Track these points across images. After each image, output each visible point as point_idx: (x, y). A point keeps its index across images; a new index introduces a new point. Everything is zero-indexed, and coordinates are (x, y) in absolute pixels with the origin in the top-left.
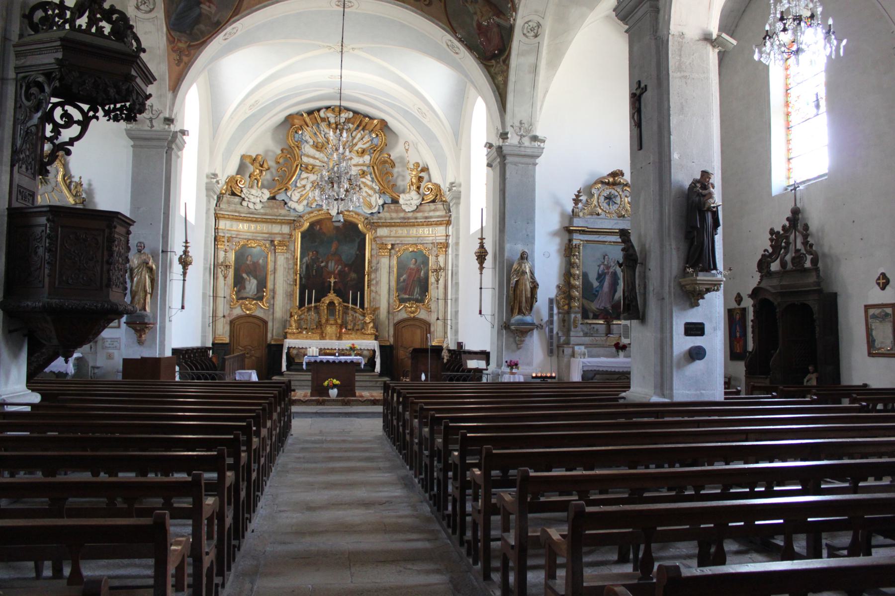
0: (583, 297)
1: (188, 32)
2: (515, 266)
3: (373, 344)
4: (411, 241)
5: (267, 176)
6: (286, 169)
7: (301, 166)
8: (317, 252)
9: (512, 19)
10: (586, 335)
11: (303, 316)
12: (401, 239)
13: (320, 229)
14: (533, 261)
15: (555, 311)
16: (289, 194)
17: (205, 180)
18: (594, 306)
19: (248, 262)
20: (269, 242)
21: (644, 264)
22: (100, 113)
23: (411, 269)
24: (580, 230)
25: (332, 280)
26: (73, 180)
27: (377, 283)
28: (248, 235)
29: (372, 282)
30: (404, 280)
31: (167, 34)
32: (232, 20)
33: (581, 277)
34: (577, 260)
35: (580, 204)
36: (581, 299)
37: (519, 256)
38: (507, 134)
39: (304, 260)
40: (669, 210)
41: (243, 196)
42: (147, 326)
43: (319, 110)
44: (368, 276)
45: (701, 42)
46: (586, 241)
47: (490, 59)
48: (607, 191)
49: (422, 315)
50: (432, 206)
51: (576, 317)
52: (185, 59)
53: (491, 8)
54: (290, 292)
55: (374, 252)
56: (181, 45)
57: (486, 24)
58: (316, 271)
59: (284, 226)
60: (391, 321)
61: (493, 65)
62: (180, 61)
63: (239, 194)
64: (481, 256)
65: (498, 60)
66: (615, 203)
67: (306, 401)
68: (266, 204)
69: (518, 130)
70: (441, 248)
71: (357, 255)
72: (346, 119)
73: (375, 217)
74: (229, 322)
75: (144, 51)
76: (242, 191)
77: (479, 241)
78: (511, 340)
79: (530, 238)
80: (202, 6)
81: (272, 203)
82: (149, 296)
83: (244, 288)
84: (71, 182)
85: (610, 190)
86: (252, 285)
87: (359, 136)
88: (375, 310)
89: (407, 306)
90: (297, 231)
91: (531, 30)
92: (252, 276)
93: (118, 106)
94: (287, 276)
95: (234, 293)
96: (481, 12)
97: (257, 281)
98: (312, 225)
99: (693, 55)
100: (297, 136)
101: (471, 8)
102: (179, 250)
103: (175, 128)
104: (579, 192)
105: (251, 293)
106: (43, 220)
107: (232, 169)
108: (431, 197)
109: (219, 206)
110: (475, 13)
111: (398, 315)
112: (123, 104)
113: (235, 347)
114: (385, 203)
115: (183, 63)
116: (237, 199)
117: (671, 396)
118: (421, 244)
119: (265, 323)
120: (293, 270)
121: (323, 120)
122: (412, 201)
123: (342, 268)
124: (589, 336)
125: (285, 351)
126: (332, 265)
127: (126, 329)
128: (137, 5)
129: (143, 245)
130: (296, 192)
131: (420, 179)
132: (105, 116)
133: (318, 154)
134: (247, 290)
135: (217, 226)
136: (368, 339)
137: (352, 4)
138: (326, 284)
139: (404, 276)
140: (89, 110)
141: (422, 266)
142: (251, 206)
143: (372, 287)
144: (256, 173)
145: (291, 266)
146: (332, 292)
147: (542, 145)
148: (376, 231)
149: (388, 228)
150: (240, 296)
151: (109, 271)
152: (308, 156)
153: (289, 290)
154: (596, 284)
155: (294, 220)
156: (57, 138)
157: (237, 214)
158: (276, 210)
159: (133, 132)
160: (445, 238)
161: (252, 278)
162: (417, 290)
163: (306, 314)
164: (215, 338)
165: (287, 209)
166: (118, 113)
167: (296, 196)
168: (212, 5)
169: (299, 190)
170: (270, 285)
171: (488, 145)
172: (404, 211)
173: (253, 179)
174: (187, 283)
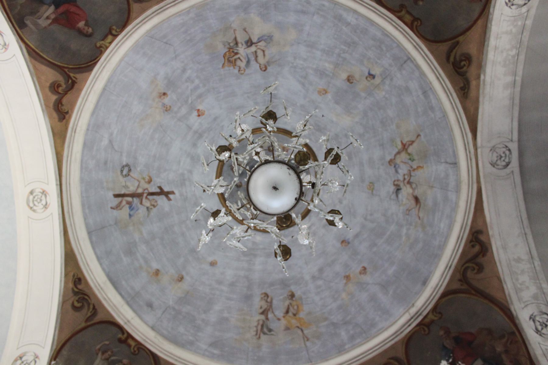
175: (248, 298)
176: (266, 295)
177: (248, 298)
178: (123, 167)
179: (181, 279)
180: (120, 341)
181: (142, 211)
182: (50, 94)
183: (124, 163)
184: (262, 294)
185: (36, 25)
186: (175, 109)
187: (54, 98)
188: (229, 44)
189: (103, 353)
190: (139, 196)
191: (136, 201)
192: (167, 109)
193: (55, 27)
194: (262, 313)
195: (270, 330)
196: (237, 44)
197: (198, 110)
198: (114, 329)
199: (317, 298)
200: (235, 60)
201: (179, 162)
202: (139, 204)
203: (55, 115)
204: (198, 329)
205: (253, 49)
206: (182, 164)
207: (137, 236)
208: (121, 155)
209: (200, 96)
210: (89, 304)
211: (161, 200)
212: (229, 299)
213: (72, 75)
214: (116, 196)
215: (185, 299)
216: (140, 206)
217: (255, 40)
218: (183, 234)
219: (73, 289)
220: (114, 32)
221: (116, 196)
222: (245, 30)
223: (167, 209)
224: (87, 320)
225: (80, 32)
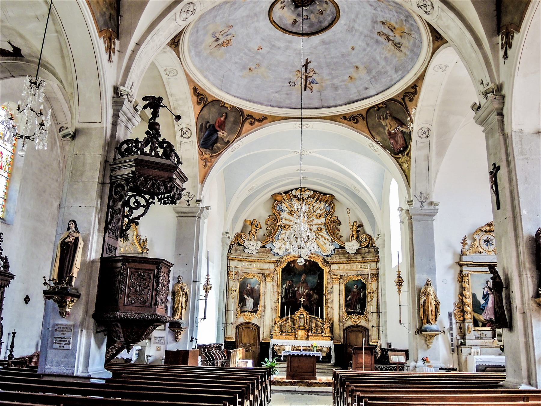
0: (474, 311)
1: (210, 148)
2: (423, 290)
3: (329, 343)
4: (353, 273)
5: (261, 232)
6: (272, 228)
7: (281, 226)
9: (410, 127)
10: (478, 338)
12: (346, 272)
13: (294, 266)
14: (435, 286)
15: (454, 321)
16: (274, 244)
17: (221, 236)
18: (482, 317)
19: (248, 288)
21: (508, 287)
22: (156, 200)
23: (354, 292)
24: (467, 264)
25: (302, 299)
26: (142, 238)
27: (332, 301)
30: (350, 299)
31: (198, 151)
32: (236, 140)
33: (471, 297)
34: (467, 285)
35: (466, 245)
36: (472, 312)
37: (425, 283)
38: (412, 201)
39: (284, 287)
40: (523, 249)
41: (245, 246)
42: (182, 329)
43: (292, 191)
44: (326, 296)
45: (535, 134)
46: (473, 271)
47: (398, 154)
48: (486, 236)
49: (363, 323)
51: (469, 325)
52: (209, 164)
53: (396, 122)
54: (274, 307)
55: (329, 281)
56: (206, 156)
57: (394, 132)
59: (270, 264)
60: (342, 327)
61: (400, 158)
62: (205, 165)
64: (399, 284)
65: (403, 154)
66: (492, 244)
67: (283, 382)
68: (259, 251)
69: (419, 198)
70: (374, 277)
71: (317, 282)
73: (329, 258)
75: (181, 163)
76: (244, 242)
77: (397, 273)
78: (423, 341)
79: (432, 271)
80: (218, 133)
81: (263, 249)
82: (184, 310)
83: (246, 305)
84: (140, 239)
85: (488, 236)
86: (250, 303)
87: (317, 205)
88: (330, 320)
89: (353, 317)
91: (424, 134)
93: (166, 195)
96: (390, 125)
98: (289, 264)
99: (531, 143)
100: (278, 207)
101: (384, 123)
102: (204, 281)
103: (202, 205)
104: (465, 238)
105: (249, 308)
106: (120, 264)
107: (238, 229)
108: (366, 244)
109: (230, 252)
110: (387, 126)
112: (169, 194)
113: (239, 344)
114: (336, 249)
115: (208, 167)
117: (537, 387)
118: (360, 275)
120: (277, 293)
121: (295, 197)
123: (308, 291)
124: (480, 339)
125: (271, 347)
126: (301, 290)
127: (169, 331)
128: (181, 134)
129: (181, 278)
130: (278, 242)
131: (357, 231)
132: (158, 202)
133: (291, 218)
134: (247, 306)
135: (229, 265)
136: (326, 340)
137: (309, 126)
140: (149, 199)
142: (250, 252)
143: (328, 304)
145: (275, 290)
146: (302, 307)
147: (437, 207)
148: (330, 267)
149: (338, 265)
150: (243, 310)
151: (156, 295)
153: (274, 306)
154: (482, 302)
155: (277, 261)
156: (131, 216)
157: (241, 257)
158: (266, 254)
159: (177, 209)
161: (250, 298)
163: (285, 322)
164: (226, 338)
165: (273, 253)
166: (166, 199)
167: (278, 245)
168: (224, 132)
169: (280, 241)
170: (261, 302)
171: (400, 209)
172: (348, 253)
173: (251, 235)
174: (207, 301)
175: (377, 42)
176: (379, 33)
177: (377, 42)
178: (290, 85)
179: (357, 67)
180: (378, 110)
181: (315, 77)
182: (255, 125)
183: (288, 84)
184: (378, 35)
185: (227, 137)
186: (258, 61)
187: (256, 123)
188: (218, 48)
189: (381, 119)
190: (307, 77)
191: (309, 79)
192: (258, 66)
193: (226, 129)
194: (389, 41)
195: (399, 44)
196: (218, 45)
197: (258, 49)
198: (371, 110)
199: (388, 15)
200: (227, 41)
201: (289, 56)
202: (311, 78)
203: (265, 121)
204: (386, 72)
205: (220, 37)
206: (290, 54)
207: (328, 82)
208: (284, 86)
209: (250, 50)
210: (356, 116)
211: (310, 66)
212: (375, 50)
213: (245, 117)
214: (305, 90)
215: (369, 71)
216: (312, 78)
217: (216, 38)
218: (332, 58)
219: (347, 121)
220: (223, 104)
221: (305, 90)
222: (210, 46)
223: (316, 64)
224: (363, 119)
225: (225, 118)
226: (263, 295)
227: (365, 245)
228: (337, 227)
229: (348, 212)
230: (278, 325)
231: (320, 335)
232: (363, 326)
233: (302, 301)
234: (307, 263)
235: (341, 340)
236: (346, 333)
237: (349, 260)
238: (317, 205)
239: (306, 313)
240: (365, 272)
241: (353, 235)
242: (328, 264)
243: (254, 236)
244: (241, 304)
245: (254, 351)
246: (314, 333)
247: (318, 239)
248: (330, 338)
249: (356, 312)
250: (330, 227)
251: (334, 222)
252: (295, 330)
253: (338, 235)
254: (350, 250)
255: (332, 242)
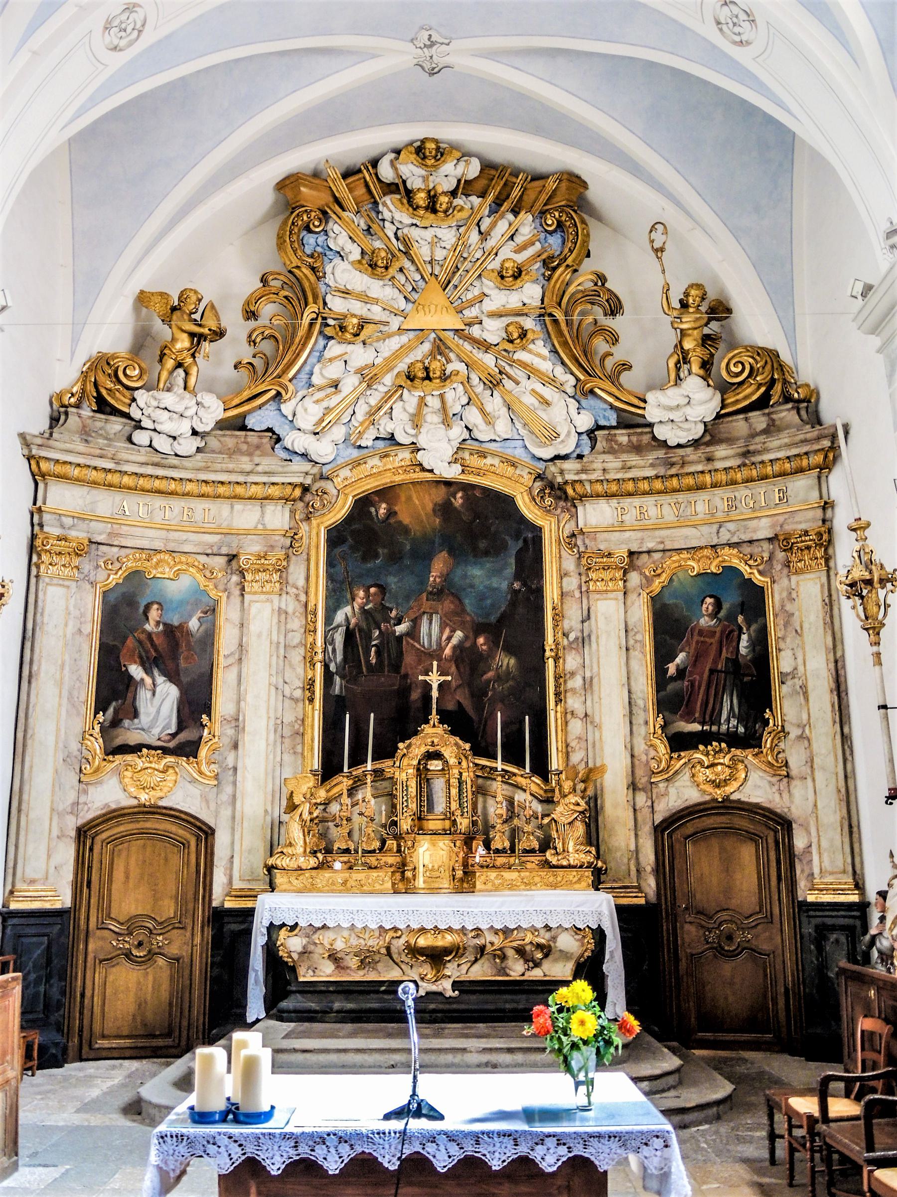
8: (383, 589)
11: (334, 808)
12: (657, 533)
13: (391, 513)
16: (287, 408)
19: (149, 627)
20: (222, 560)
23: (701, 632)
25: (434, 679)
27: (588, 685)
28: (152, 539)
29: (570, 684)
30: (681, 673)
39: (340, 617)
41: (135, 413)
44: (556, 659)
50: (759, 420)
54: (291, 725)
55: (571, 584)
58: (378, 653)
59: (270, 508)
60: (644, 814)
63: (126, 410)
70: (808, 548)
71: (516, 592)
72: (459, 181)
73: (567, 465)
74: (73, 834)
76: (134, 400)
81: (231, 439)
83: (136, 714)
89: (701, 763)
90: (314, 522)
92: (164, 673)
94: (281, 672)
95: (97, 728)
97: (181, 689)
98: (363, 504)
105: (156, 731)
111: (666, 794)
116: (116, 425)
118: (730, 545)
119: (206, 833)
120: (302, 651)
121: (391, 188)
122: (688, 410)
123: (466, 637)
125: (259, 939)
133: (376, 288)
134: (144, 719)
135: (39, 503)
136: (569, 885)
138: (415, 695)
139: (681, 658)
141: (740, 619)
142: (162, 443)
144: (179, 346)
146: (434, 717)
149: (614, 502)
150: (118, 742)
152: (346, 293)
153: (289, 718)
155: (306, 489)
160: (819, 513)
161: (160, 679)
162: (729, 704)
163: (346, 800)
164: (12, 892)
169: (320, 395)
172: (664, 444)
173: (170, 363)
226: (231, 660)
227: (746, 398)
228: (601, 317)
229: (657, 245)
230: (306, 816)
231: (536, 859)
232: (757, 806)
233: (435, 686)
234: (458, 500)
235: (643, 884)
236: (671, 847)
237: (673, 471)
238: (502, 226)
239: (456, 744)
240: (755, 531)
241: (684, 358)
242: (562, 503)
243: (187, 373)
244: (111, 711)
245: (178, 960)
246: (504, 851)
247: (507, 383)
248: (588, 873)
249: (718, 733)
250: (569, 323)
251: (591, 297)
252: (398, 837)
253: (609, 363)
254: (670, 425)
255: (582, 393)
